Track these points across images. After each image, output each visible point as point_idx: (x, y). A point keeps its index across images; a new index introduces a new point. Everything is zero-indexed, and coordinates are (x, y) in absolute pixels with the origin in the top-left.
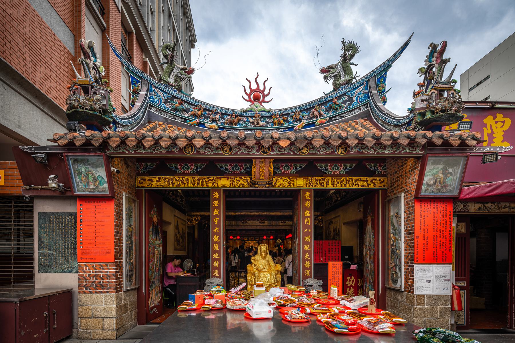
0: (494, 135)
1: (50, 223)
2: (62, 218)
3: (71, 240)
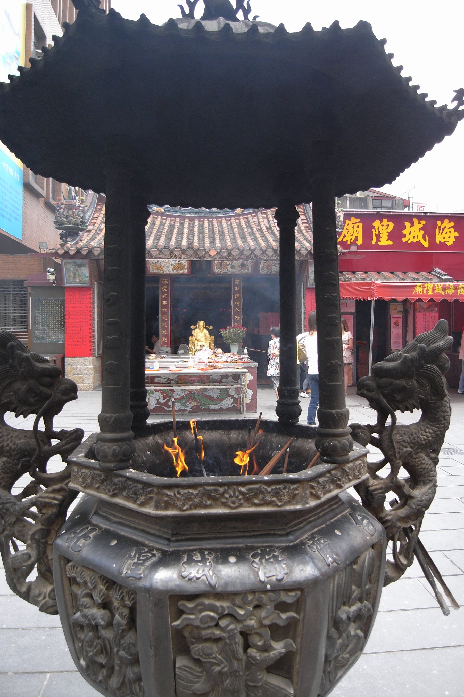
1: (42, 306)
2: (52, 303)
3: (58, 318)
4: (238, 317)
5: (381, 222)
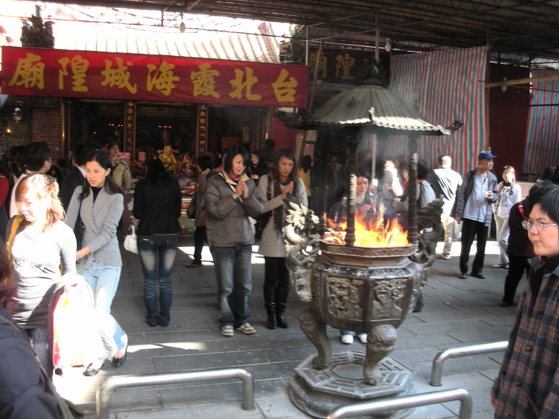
0: (344, 70)
4: (203, 142)
5: (344, 56)
